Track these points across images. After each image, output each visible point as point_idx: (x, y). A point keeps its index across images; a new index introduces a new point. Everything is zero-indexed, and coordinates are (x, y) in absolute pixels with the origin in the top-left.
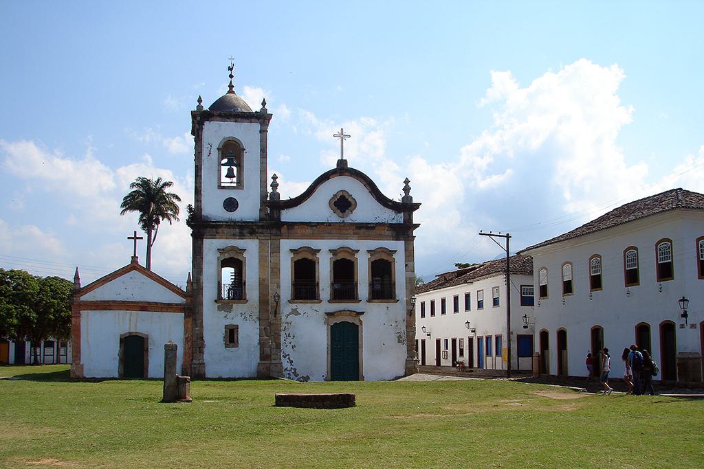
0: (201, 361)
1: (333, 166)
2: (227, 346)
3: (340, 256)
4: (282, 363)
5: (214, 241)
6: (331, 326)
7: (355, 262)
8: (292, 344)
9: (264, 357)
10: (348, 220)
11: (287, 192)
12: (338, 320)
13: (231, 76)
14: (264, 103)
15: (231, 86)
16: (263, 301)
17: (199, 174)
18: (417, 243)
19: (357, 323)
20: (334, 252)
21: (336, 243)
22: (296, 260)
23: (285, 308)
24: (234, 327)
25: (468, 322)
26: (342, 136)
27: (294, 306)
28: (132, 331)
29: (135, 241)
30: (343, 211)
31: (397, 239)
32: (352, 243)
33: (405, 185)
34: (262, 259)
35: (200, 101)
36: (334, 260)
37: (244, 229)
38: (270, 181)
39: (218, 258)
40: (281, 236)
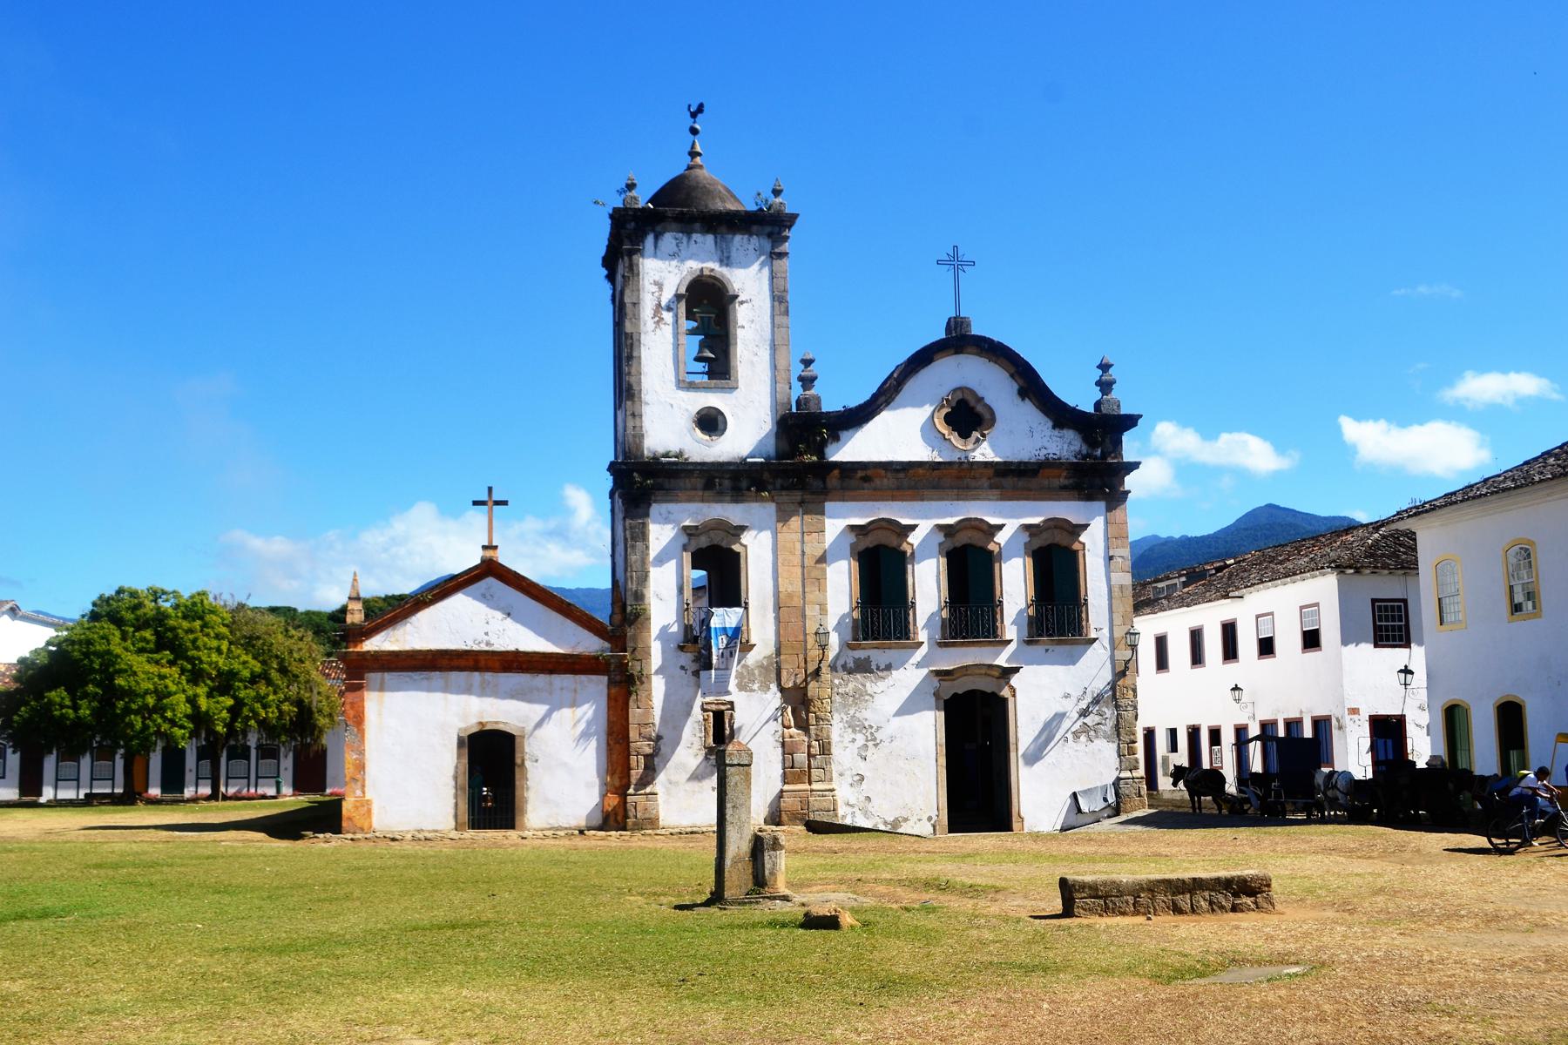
6: (945, 701)
11: (833, 398)
12: (962, 685)
22: (862, 547)
25: (1236, 688)
26: (956, 262)
29: (490, 511)
32: (987, 511)
33: (1100, 372)
36: (950, 545)
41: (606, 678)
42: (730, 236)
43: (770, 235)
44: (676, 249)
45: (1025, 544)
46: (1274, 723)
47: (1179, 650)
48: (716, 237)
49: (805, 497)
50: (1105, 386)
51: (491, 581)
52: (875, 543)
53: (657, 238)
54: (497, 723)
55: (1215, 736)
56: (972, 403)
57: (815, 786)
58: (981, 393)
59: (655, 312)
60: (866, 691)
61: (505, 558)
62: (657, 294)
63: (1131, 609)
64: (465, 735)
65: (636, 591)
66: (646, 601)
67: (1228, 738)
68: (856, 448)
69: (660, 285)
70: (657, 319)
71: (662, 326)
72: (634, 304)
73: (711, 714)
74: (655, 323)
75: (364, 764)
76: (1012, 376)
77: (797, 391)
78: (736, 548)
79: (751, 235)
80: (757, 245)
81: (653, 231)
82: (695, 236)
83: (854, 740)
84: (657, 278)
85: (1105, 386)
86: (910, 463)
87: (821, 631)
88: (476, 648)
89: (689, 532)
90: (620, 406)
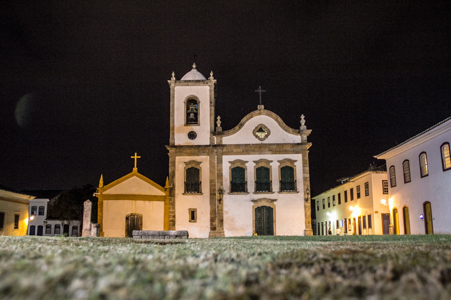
6: (255, 209)
12: (260, 204)
21: (257, 157)
22: (232, 167)
32: (268, 157)
37: (200, 149)
39: (185, 168)
41: (163, 203)
58: (266, 126)
64: (128, 216)
87: (220, 189)
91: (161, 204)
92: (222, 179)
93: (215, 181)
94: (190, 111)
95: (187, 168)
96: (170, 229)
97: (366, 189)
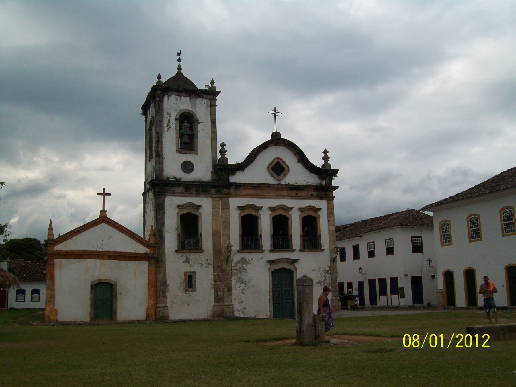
0: (164, 305)
1: (268, 138)
2: (186, 290)
3: (278, 213)
4: (233, 305)
5: (174, 198)
6: (272, 272)
7: (289, 217)
8: (242, 287)
9: (218, 299)
10: (283, 182)
13: (179, 60)
14: (212, 83)
15: (179, 68)
16: (217, 250)
17: (160, 140)
18: (336, 202)
19: (292, 268)
20: (272, 209)
21: (275, 202)
22: (243, 215)
23: (236, 257)
24: (192, 274)
25: (360, 268)
27: (242, 255)
28: (101, 278)
30: (279, 175)
31: (321, 198)
32: (288, 203)
33: (324, 155)
34: (215, 214)
35: (159, 77)
36: (274, 215)
38: (219, 148)
39: (178, 213)
40: (229, 195)
41: (148, 262)
42: (195, 98)
43: (210, 99)
44: (176, 102)
45: (300, 215)
46: (374, 280)
47: (349, 253)
48: (190, 98)
49: (222, 195)
50: (326, 158)
51: (104, 225)
52: (247, 213)
53: (168, 97)
54: (106, 279)
55: (350, 285)
56: (281, 163)
57: (225, 304)
59: (167, 124)
60: (244, 268)
61: (113, 216)
62: (168, 118)
63: (335, 239)
64: (94, 284)
65: (160, 229)
66: (164, 233)
67: (355, 286)
68: (238, 178)
69: (169, 115)
70: (168, 127)
71: (170, 130)
72: (160, 121)
73: (187, 276)
74: (167, 128)
75: (54, 295)
76: (295, 154)
77: (219, 156)
78: (197, 214)
79: (203, 98)
80: (205, 102)
81: (167, 94)
82: (182, 97)
83: (240, 287)
84: (168, 112)
85: (326, 158)
86: (260, 184)
88: (98, 250)
89: (180, 207)
90: (150, 160)
91: (144, 266)
92: (229, 230)
93: (220, 233)
94: (183, 131)
95: (181, 213)
96: (158, 302)
97: (392, 247)
